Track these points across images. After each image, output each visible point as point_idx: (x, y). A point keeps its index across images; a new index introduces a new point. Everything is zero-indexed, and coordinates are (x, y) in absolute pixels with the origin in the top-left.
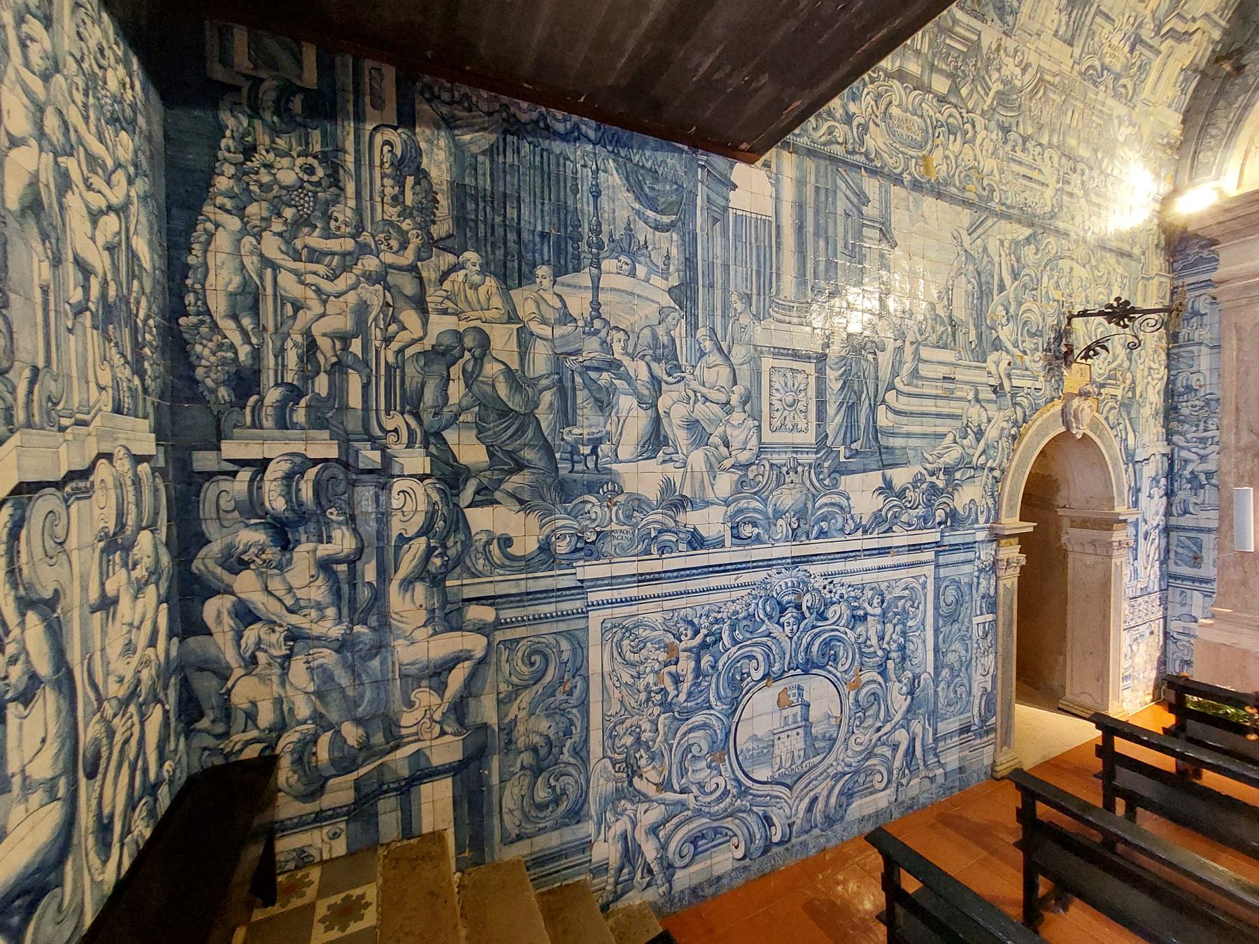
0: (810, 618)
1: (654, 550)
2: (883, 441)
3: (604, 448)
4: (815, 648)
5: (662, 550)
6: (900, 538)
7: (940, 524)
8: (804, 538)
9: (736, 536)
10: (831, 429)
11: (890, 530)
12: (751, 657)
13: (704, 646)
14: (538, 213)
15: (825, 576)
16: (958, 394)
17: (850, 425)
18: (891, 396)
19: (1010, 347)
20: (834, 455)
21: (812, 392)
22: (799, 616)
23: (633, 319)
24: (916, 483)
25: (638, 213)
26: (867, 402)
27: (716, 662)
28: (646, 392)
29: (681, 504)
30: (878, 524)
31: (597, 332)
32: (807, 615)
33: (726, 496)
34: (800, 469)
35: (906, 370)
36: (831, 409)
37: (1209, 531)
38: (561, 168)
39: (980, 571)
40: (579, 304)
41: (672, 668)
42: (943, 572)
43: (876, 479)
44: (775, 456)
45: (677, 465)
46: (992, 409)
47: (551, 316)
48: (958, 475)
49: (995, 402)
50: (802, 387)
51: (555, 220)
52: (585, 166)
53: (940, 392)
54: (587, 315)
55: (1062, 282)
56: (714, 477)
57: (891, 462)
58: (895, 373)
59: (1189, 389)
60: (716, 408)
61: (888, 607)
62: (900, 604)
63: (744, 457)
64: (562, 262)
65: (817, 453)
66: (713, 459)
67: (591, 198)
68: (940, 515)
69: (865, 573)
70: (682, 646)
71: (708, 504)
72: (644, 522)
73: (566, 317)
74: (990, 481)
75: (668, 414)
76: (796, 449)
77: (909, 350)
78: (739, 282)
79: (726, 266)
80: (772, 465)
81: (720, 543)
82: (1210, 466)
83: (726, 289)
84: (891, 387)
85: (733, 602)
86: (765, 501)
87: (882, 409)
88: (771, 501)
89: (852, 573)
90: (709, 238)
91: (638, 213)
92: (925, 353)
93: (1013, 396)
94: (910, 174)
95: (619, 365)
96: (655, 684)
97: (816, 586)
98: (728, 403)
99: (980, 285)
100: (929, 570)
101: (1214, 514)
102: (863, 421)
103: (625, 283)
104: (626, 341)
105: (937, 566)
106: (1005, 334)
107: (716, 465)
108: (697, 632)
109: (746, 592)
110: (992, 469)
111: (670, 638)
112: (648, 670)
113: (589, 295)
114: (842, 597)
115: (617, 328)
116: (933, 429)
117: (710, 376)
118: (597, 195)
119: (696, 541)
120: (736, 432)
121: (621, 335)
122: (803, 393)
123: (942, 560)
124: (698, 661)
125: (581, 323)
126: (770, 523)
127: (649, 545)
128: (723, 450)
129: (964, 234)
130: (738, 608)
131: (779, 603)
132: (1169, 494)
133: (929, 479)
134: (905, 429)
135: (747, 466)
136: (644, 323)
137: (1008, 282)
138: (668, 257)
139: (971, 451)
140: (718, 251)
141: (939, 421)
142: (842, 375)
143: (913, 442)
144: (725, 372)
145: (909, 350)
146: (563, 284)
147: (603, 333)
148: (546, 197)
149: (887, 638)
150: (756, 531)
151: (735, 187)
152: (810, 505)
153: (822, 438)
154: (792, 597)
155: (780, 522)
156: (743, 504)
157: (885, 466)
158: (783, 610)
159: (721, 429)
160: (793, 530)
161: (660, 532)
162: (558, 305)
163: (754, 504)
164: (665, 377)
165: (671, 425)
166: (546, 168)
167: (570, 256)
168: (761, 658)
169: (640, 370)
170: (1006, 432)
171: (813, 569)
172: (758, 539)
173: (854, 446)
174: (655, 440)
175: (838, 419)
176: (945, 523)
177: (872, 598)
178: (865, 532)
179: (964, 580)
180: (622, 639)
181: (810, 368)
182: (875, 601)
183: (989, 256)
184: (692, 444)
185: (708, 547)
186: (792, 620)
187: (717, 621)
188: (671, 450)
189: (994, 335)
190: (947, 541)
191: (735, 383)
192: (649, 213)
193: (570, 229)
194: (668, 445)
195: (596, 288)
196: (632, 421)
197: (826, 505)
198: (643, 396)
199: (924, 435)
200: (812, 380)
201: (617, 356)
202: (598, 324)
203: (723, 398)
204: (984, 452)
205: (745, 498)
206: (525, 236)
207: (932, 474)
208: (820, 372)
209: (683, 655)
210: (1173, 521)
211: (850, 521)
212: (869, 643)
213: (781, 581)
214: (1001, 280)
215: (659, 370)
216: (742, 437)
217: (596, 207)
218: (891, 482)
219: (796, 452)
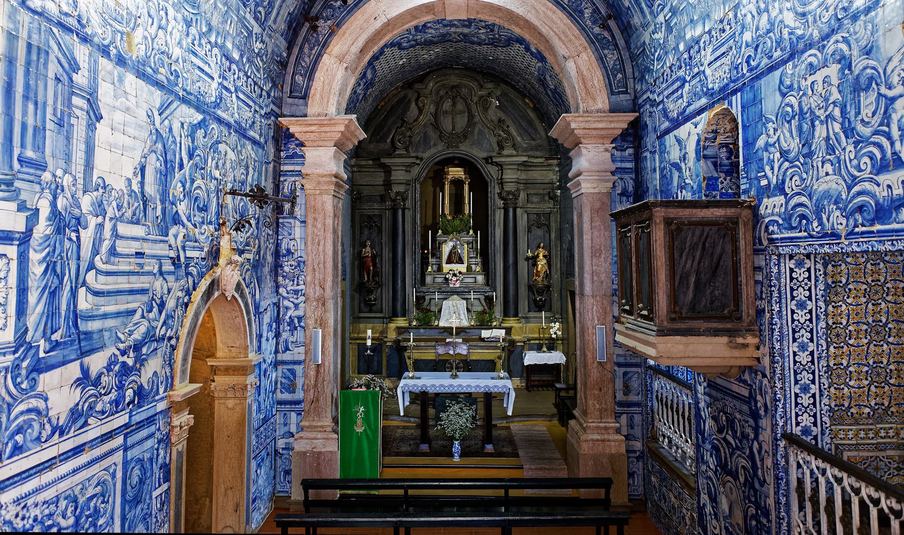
2: (83, 326)
6: (95, 430)
7: (128, 404)
11: (86, 424)
15: (17, 501)
17: (51, 313)
18: (91, 277)
19: (185, 220)
35: (106, 246)
36: (32, 297)
37: (298, 363)
42: (130, 454)
43: (73, 370)
48: (144, 350)
55: (220, 163)
57: (88, 348)
59: (289, 252)
61: (82, 512)
65: (15, 352)
82: (300, 313)
84: (91, 266)
87: (82, 291)
89: (48, 485)
92: (123, 229)
93: (187, 266)
94: (116, 47)
99: (166, 162)
101: (302, 350)
102: (64, 307)
105: (126, 450)
106: (182, 208)
110: (170, 338)
123: (130, 441)
129: (156, 113)
132: (278, 335)
133: (121, 359)
134: (103, 310)
137: (185, 161)
139: (154, 324)
141: (130, 298)
142: (45, 258)
143: (110, 323)
145: (108, 226)
170: (181, 300)
173: (56, 337)
175: (40, 308)
178: (61, 434)
179: (147, 456)
183: (173, 137)
189: (175, 210)
197: (22, 413)
199: (118, 314)
200: (14, 265)
204: (164, 323)
207: (124, 353)
208: (23, 259)
210: (280, 357)
214: (181, 159)
218: (88, 369)
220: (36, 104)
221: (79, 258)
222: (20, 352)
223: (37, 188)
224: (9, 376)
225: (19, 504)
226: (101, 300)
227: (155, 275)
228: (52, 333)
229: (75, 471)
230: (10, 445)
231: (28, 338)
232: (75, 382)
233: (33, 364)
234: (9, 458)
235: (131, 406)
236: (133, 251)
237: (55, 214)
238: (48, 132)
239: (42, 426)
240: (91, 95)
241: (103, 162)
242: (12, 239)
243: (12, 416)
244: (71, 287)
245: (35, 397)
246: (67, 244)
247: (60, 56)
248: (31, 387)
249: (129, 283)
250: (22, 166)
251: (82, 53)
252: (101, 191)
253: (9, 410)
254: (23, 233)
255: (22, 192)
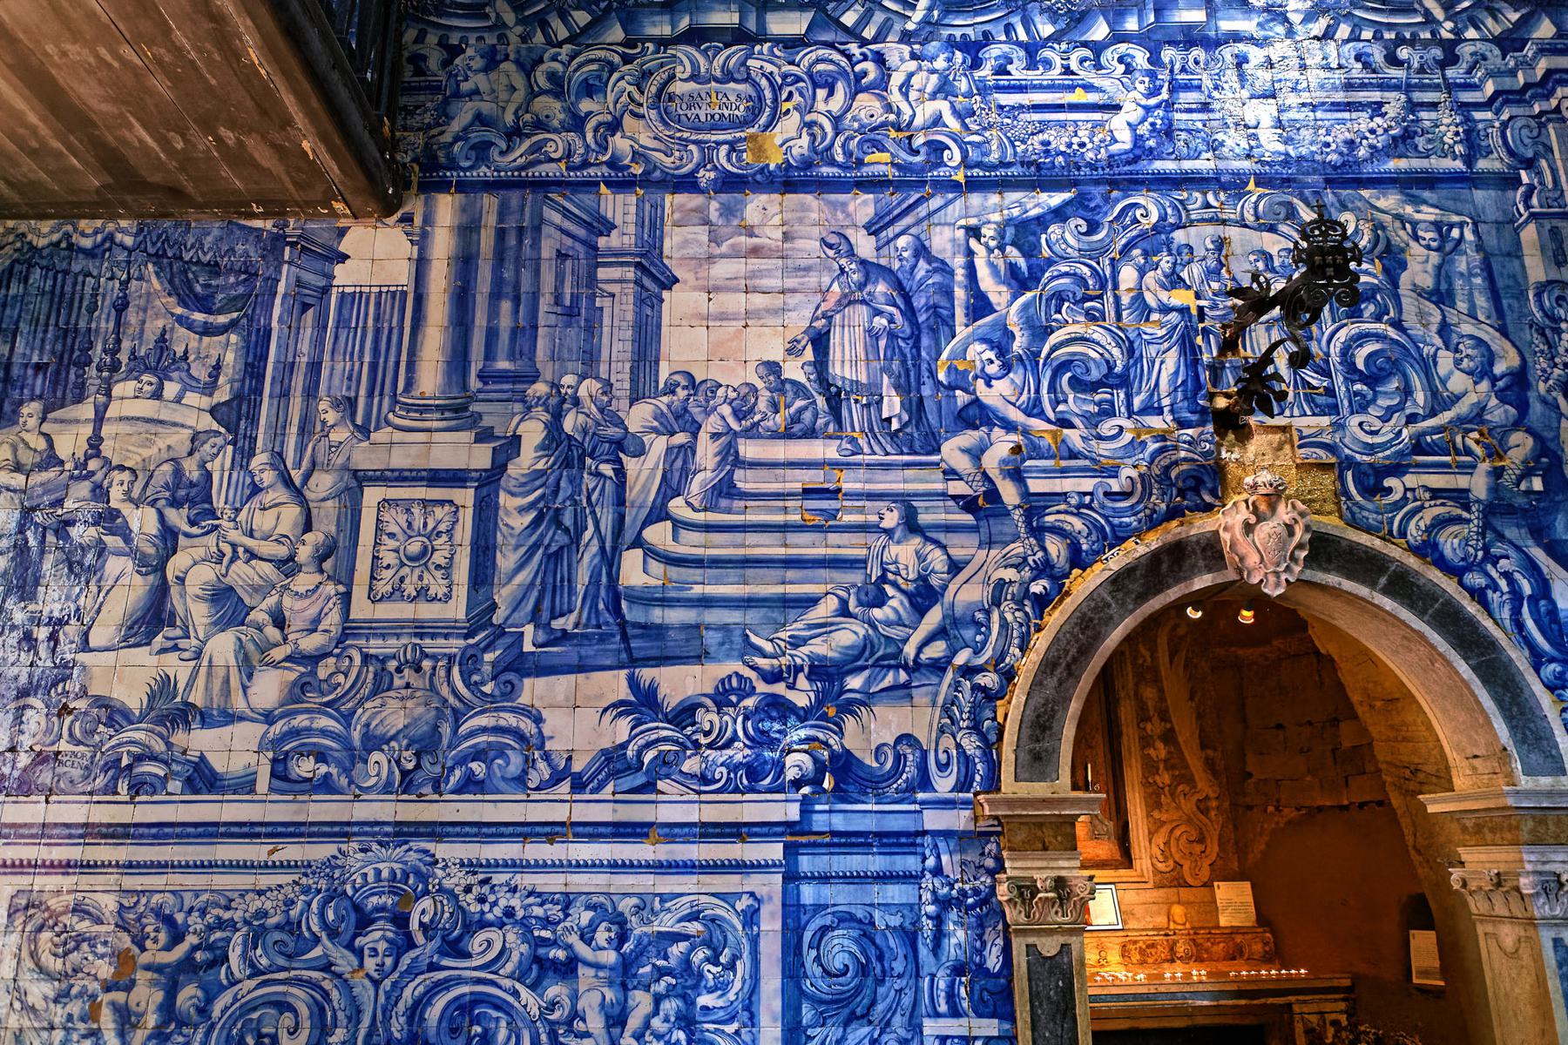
0: (426, 948)
1: (123, 787)
2: (631, 613)
3: (72, 630)
4: (433, 1013)
5: (136, 788)
8: (427, 789)
9: (280, 773)
10: (503, 596)
12: (283, 1006)
13: (188, 966)
14: (38, 342)
15: (471, 866)
16: (848, 518)
20: (507, 640)
21: (465, 532)
22: (400, 940)
23: (146, 453)
24: (722, 697)
25: (180, 320)
26: (594, 548)
27: (210, 1000)
28: (151, 550)
29: (184, 716)
30: (615, 775)
31: (93, 473)
32: (420, 939)
33: (268, 707)
34: (427, 664)
36: (506, 561)
38: (79, 288)
39: (944, 904)
40: (70, 444)
41: (120, 997)
43: (615, 684)
44: (372, 642)
45: (186, 655)
46: (962, 546)
47: (27, 458)
49: (973, 529)
50: (442, 527)
51: (59, 347)
52: (111, 279)
53: (795, 518)
54: (80, 455)
56: (250, 676)
58: (671, 487)
60: (267, 569)
62: (677, 950)
63: (310, 643)
64: (59, 394)
65: (466, 637)
66: (251, 647)
67: (113, 312)
68: (797, 763)
69: (584, 871)
70: (145, 958)
71: (230, 718)
72: (113, 742)
73: (51, 459)
74: (966, 696)
75: (181, 580)
76: (422, 629)
77: (707, 452)
78: (336, 381)
79: (315, 367)
80: (366, 658)
81: (246, 785)
83: (311, 393)
84: (658, 513)
85: (260, 893)
86: (347, 719)
88: (362, 716)
90: (294, 330)
91: (180, 320)
92: (749, 450)
95: (114, 514)
96: (83, 1020)
97: (447, 883)
98: (291, 558)
100: (770, 885)
102: (583, 577)
103: (146, 408)
104: (132, 483)
105: (792, 877)
107: (255, 657)
108: (177, 937)
109: (289, 879)
110: (968, 671)
111: (126, 941)
112: (74, 991)
113: (88, 430)
114: (509, 912)
115: (122, 468)
116: (779, 589)
117: (264, 522)
118: (121, 307)
119: (202, 779)
120: (299, 605)
121: (126, 476)
122: (444, 538)
123: (806, 863)
124: (171, 992)
125: (68, 466)
126: (354, 757)
127: (115, 779)
128: (272, 633)
130: (268, 905)
131: (357, 908)
134: (698, 590)
135: (314, 659)
136: (165, 456)
138: (218, 367)
140: (305, 346)
141: (791, 574)
142: (532, 505)
143: (714, 616)
144: (292, 513)
146: (56, 421)
147: (99, 476)
148: (52, 321)
149: (634, 1022)
150: (323, 769)
151: (344, 258)
152: (446, 730)
153: (481, 616)
154: (388, 900)
155: (376, 756)
156: (301, 721)
157: (633, 662)
158: (364, 922)
159: (271, 601)
160: (405, 773)
161: (139, 759)
162: (42, 444)
163: (324, 722)
164: (186, 528)
165: (183, 595)
166: (58, 291)
167: (70, 386)
168: (304, 1011)
169: (143, 521)
171: (442, 850)
172: (326, 785)
173: (557, 624)
174: (153, 619)
176: (817, 782)
177: (593, 927)
178: (579, 785)
180: (40, 929)
181: (466, 497)
182: (601, 936)
184: (215, 624)
185: (222, 790)
186: (382, 946)
187: (221, 924)
188: (178, 632)
190: (819, 822)
191: (308, 527)
192: (199, 317)
193: (77, 353)
194: (172, 625)
195: (100, 419)
196: (125, 588)
197: (484, 730)
198: (144, 555)
200: (467, 516)
201: (113, 504)
202: (93, 465)
203: (282, 551)
205: (307, 711)
206: (15, 371)
207: (773, 677)
209: (142, 976)
211: (541, 765)
212: (579, 1026)
213: (367, 866)
215: (178, 518)
216: (312, 612)
217: (118, 324)
219: (421, 636)
220: (517, 300)
221: (620, 501)
222: (477, 638)
223: (518, 407)
224: (456, 670)
225: (475, 873)
226: (674, 572)
227: (889, 532)
228: (554, 617)
229: (616, 867)
230: (458, 773)
231: (498, 618)
232: (614, 706)
233: (509, 659)
234: (453, 792)
235: (806, 790)
236: (798, 487)
237: (555, 437)
238: (541, 331)
239: (529, 763)
240: (641, 256)
241: (683, 346)
242: (465, 480)
243: (463, 729)
244: (602, 549)
245: (513, 710)
246: (589, 481)
247: (568, 225)
248: (503, 694)
249: (786, 546)
250: (486, 383)
251: (620, 207)
252: (682, 393)
253: (457, 720)
254: (485, 470)
255: (485, 418)
